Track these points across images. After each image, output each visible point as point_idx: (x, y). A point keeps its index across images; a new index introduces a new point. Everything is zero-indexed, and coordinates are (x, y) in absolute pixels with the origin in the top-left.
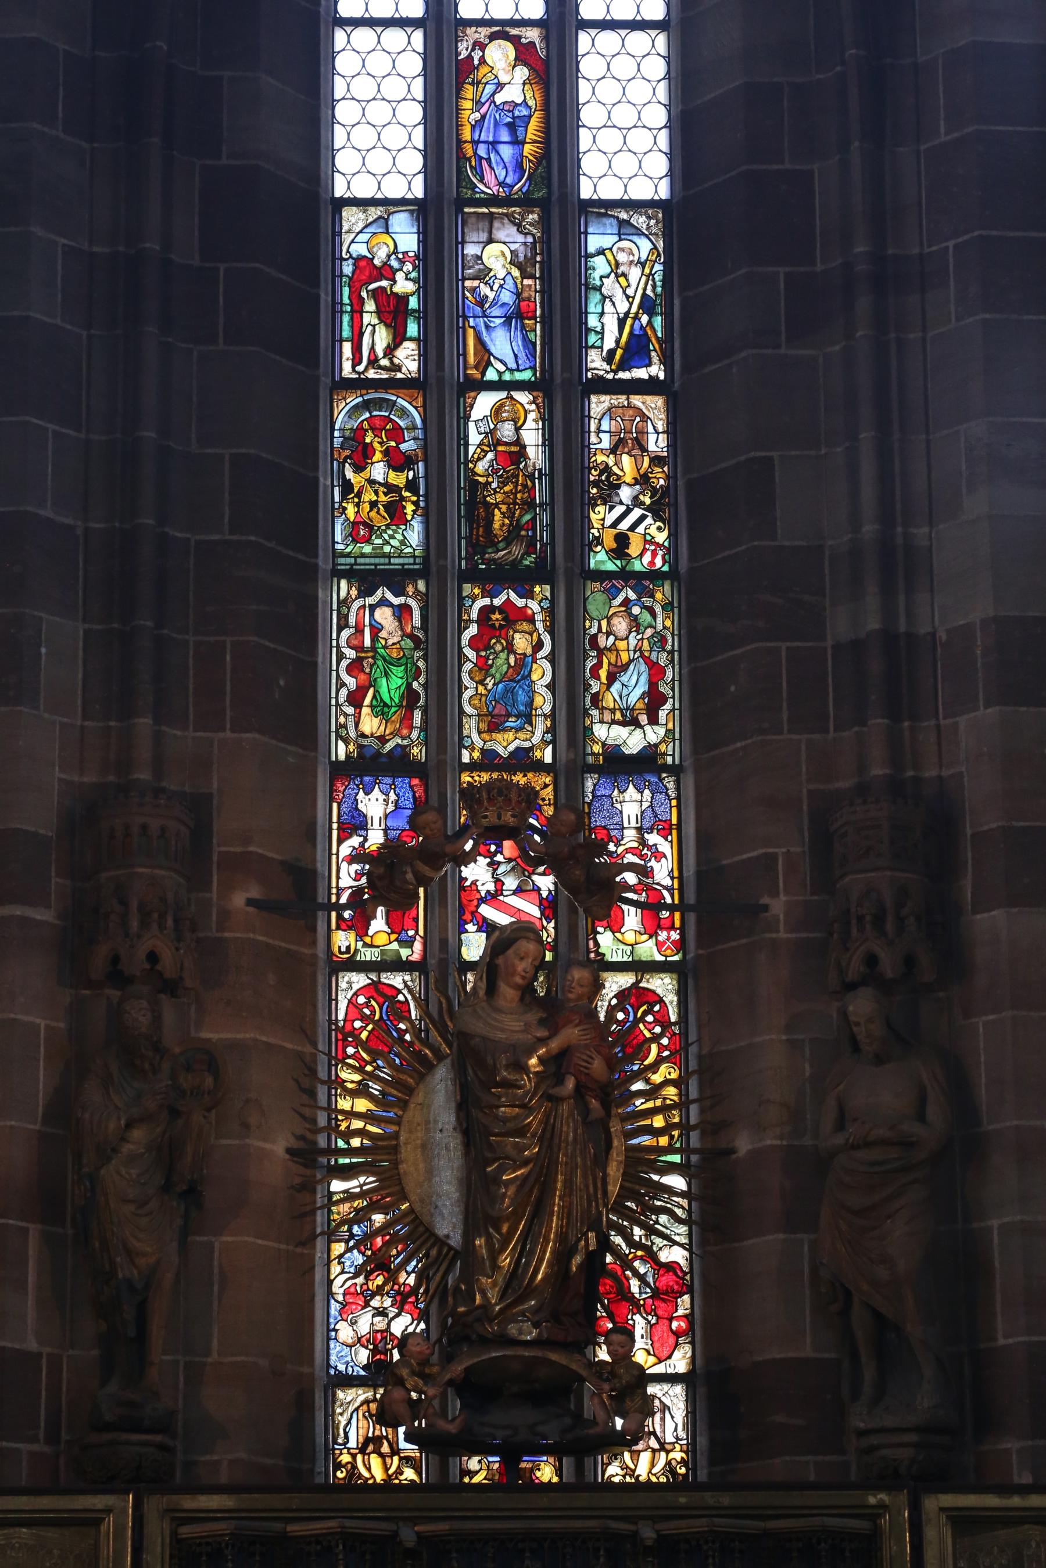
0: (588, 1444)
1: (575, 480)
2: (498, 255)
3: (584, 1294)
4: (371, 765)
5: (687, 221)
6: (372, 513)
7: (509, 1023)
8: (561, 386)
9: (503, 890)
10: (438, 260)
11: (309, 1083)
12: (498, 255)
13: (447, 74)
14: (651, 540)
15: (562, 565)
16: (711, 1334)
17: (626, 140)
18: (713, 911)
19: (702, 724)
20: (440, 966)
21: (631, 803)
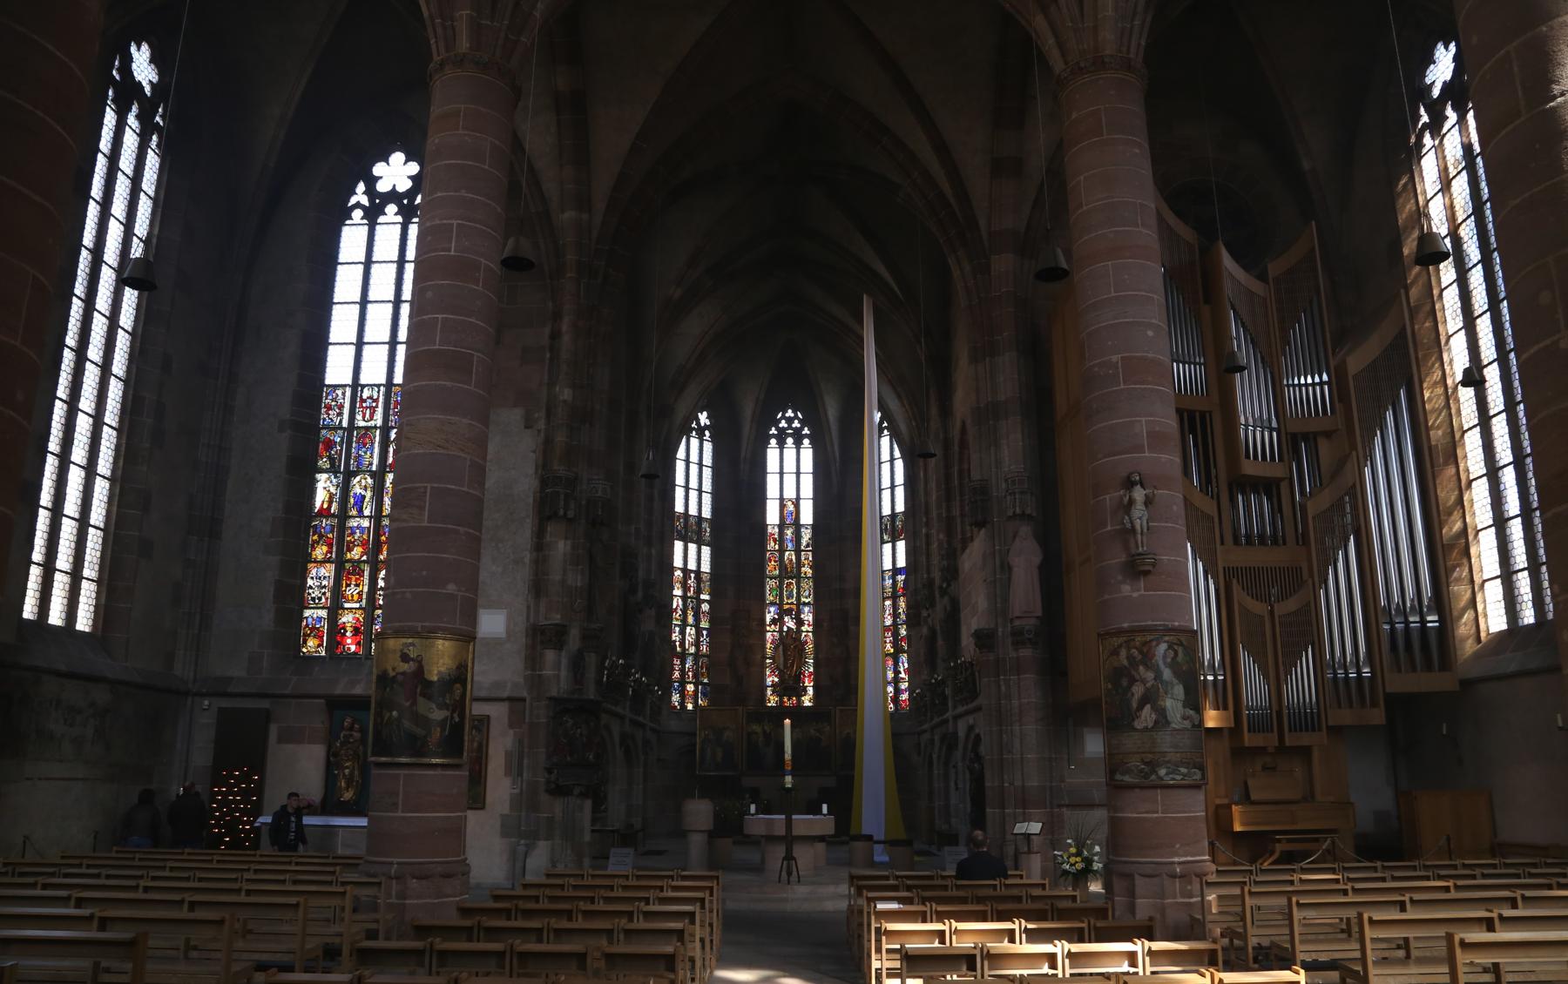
0: (799, 696)
1: (799, 564)
2: (789, 532)
3: (798, 678)
4: (772, 604)
5: (814, 527)
6: (772, 568)
7: (790, 641)
8: (798, 551)
9: (790, 623)
10: (781, 533)
11: (764, 647)
12: (789, 532)
13: (782, 506)
14: (809, 572)
15: (798, 577)
16: (815, 681)
17: (807, 517)
18: (817, 624)
19: (815, 599)
20: (781, 631)
21: (806, 609)
